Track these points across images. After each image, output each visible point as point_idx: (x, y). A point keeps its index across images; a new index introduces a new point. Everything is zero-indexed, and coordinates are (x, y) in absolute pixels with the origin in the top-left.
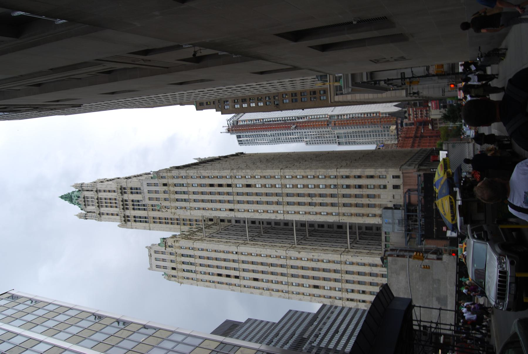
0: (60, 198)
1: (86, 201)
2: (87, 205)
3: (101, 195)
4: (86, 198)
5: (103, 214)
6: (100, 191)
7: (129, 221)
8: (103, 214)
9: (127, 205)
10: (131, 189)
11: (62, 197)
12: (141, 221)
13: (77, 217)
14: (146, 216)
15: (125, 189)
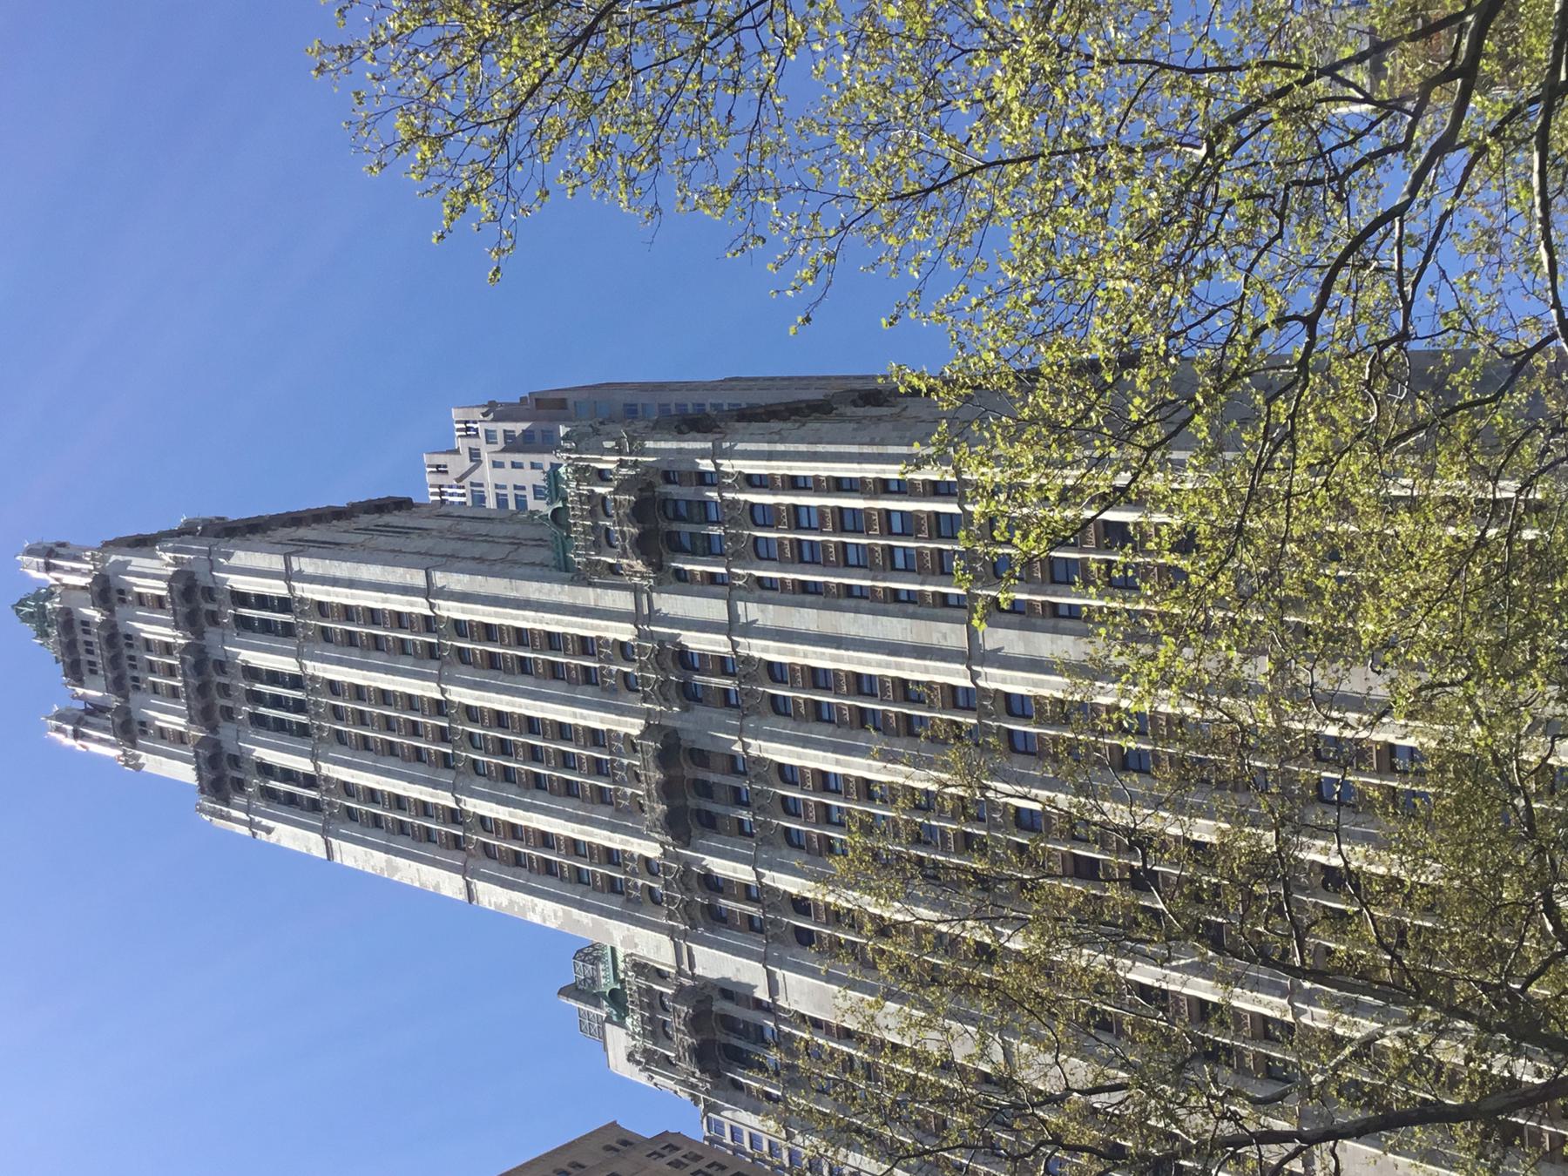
2: (85, 668)
7: (239, 786)
9: (225, 690)
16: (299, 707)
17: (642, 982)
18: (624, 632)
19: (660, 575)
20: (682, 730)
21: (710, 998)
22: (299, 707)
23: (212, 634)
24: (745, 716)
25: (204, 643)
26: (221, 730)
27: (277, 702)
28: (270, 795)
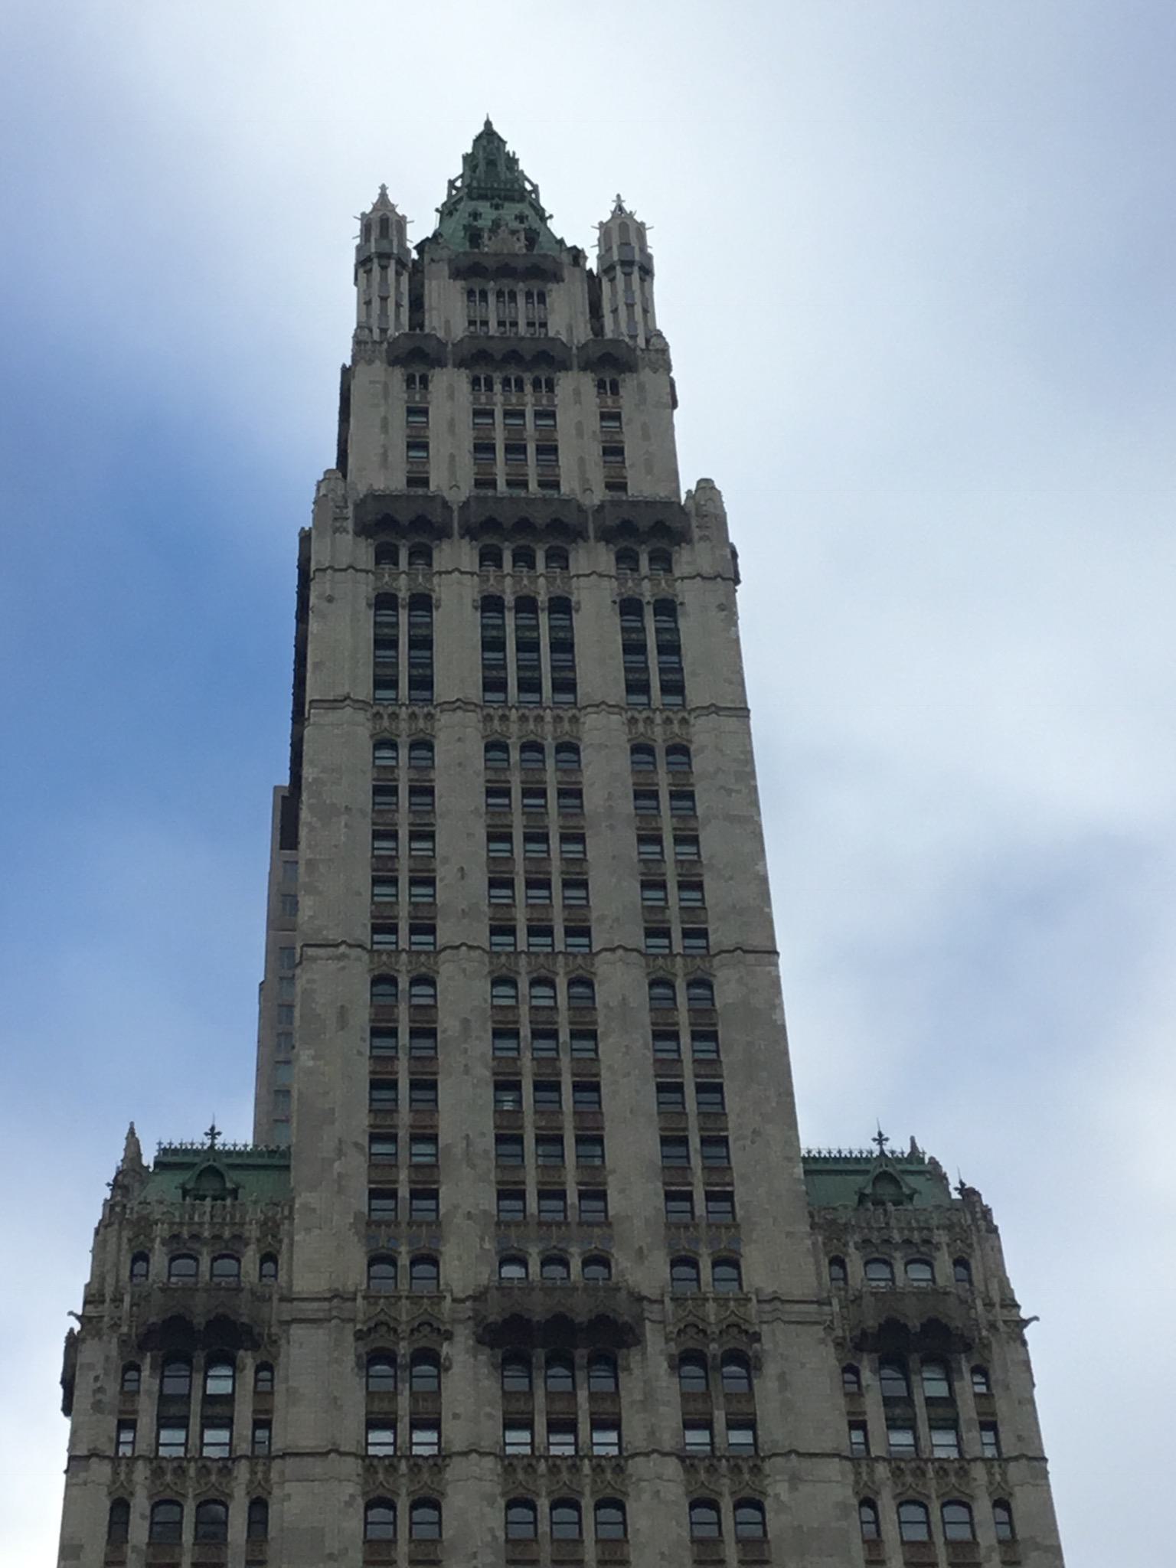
0: (480, 128)
1: (506, 284)
2: (477, 284)
3: (577, 393)
4: (535, 286)
5: (418, 382)
6: (609, 388)
7: (385, 555)
8: (418, 382)
9: (525, 558)
10: (667, 608)
11: (489, 141)
12: (385, 642)
13: (375, 198)
14: (444, 688)
15: (663, 560)
16: (529, 685)
17: (253, 1232)
18: (757, 1273)
19: (850, 1345)
20: (644, 1354)
21: (255, 1346)
22: (529, 685)
23: (604, 557)
24: (682, 1459)
25: (592, 541)
26: (467, 538)
27: (528, 646)
28: (385, 602)
